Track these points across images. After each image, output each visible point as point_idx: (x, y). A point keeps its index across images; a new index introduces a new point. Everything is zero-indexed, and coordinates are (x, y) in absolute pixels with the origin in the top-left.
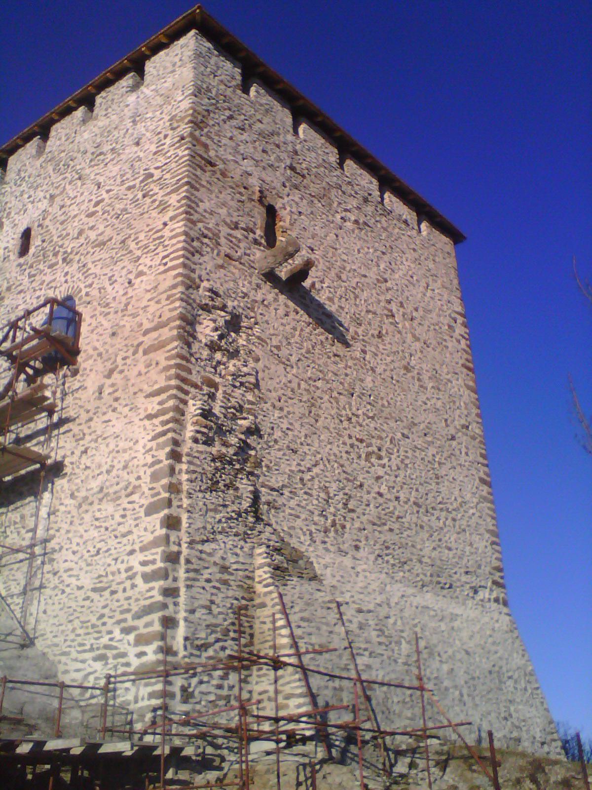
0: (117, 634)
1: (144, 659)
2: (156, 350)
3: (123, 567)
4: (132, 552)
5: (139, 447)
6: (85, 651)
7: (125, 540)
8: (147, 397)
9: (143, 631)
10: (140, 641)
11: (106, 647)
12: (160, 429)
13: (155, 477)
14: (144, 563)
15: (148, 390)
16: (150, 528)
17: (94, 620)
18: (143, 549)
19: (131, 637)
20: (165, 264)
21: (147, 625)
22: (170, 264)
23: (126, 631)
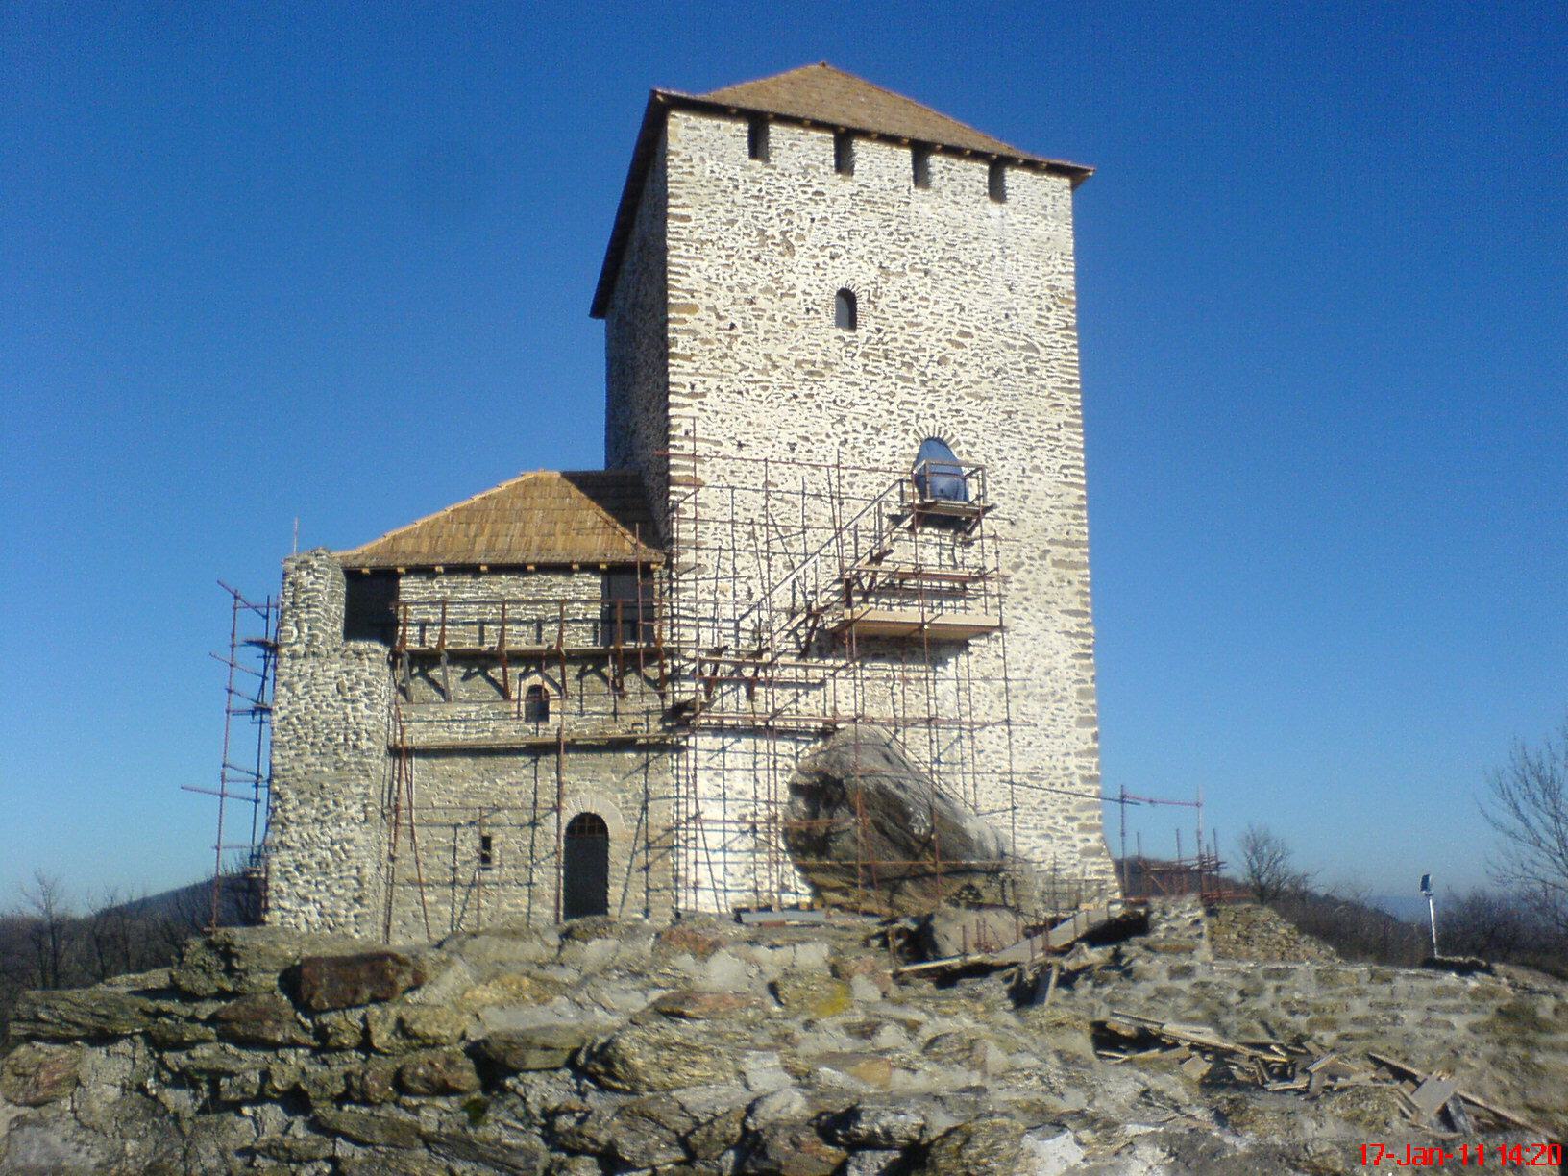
0: (1060, 818)
1: (1089, 844)
2: (1067, 568)
3: (1059, 765)
4: (1068, 754)
5: (1062, 656)
6: (1028, 828)
7: (1058, 741)
8: (1062, 612)
9: (1083, 821)
10: (1083, 828)
11: (1049, 828)
12: (1080, 650)
13: (1082, 693)
14: (1080, 767)
15: (1066, 607)
16: (1083, 738)
17: (1034, 803)
18: (1079, 754)
19: (1075, 825)
20: (1066, 475)
21: (1088, 818)
22: (1071, 479)
23: (1071, 819)
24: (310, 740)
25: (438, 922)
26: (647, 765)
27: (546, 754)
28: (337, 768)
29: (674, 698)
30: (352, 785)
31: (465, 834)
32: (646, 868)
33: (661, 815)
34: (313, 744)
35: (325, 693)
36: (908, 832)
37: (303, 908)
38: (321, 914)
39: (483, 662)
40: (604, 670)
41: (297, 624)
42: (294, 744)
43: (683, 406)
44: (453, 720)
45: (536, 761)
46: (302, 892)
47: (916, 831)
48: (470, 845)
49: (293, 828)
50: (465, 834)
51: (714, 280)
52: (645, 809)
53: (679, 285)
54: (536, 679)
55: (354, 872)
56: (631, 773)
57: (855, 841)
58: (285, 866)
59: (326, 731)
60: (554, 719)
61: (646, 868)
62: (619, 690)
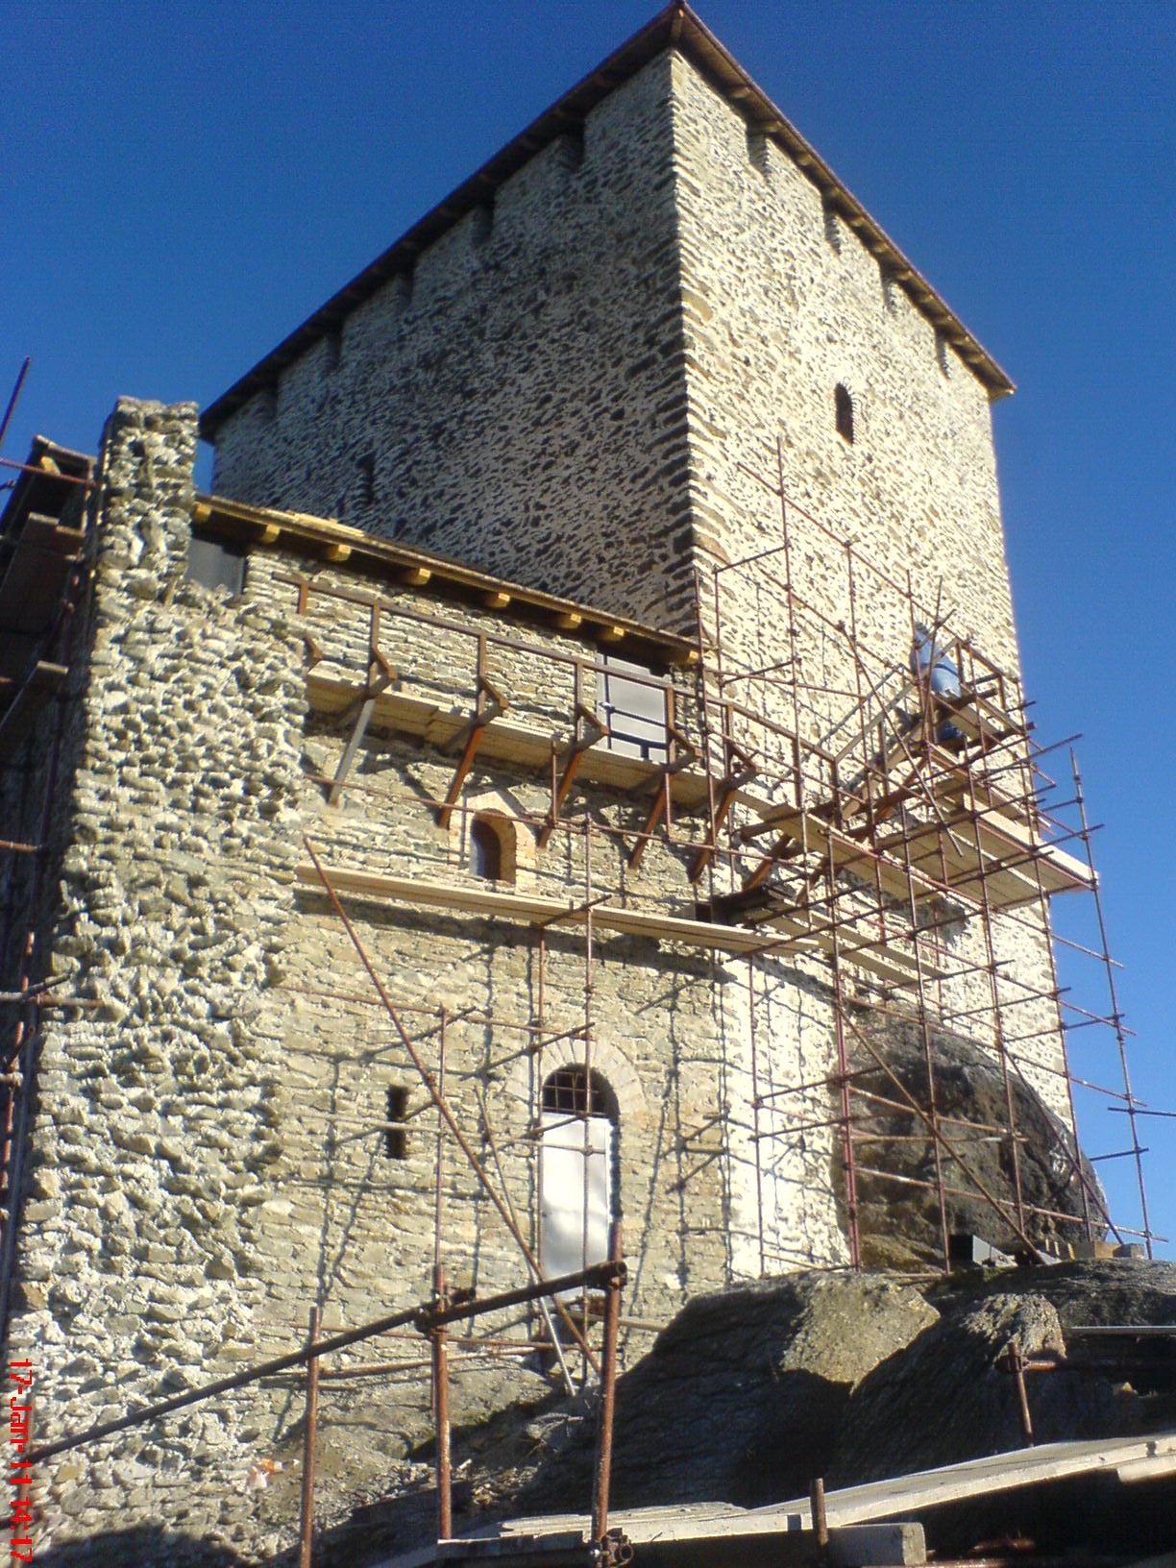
24: (171, 773)
25: (294, 1264)
26: (674, 994)
27: (510, 944)
28: (227, 850)
29: (712, 885)
30: (253, 895)
31: (355, 1077)
32: (680, 1186)
33: (697, 1089)
34: (176, 783)
35: (210, 680)
36: (1043, 1168)
37: (129, 1168)
38: (173, 1187)
39: (402, 746)
40: (604, 811)
41: (142, 529)
42: (136, 771)
43: (706, 439)
44: (341, 843)
45: (490, 952)
46: (129, 1127)
47: (1055, 1167)
48: (365, 1105)
49: (114, 967)
50: (355, 1077)
51: (726, 287)
52: (674, 1074)
53: (692, 270)
54: (491, 801)
55: (254, 1095)
56: (651, 1004)
57: (967, 1178)
58: (82, 1057)
59: (205, 763)
60: (524, 879)
61: (680, 1186)
62: (632, 857)
